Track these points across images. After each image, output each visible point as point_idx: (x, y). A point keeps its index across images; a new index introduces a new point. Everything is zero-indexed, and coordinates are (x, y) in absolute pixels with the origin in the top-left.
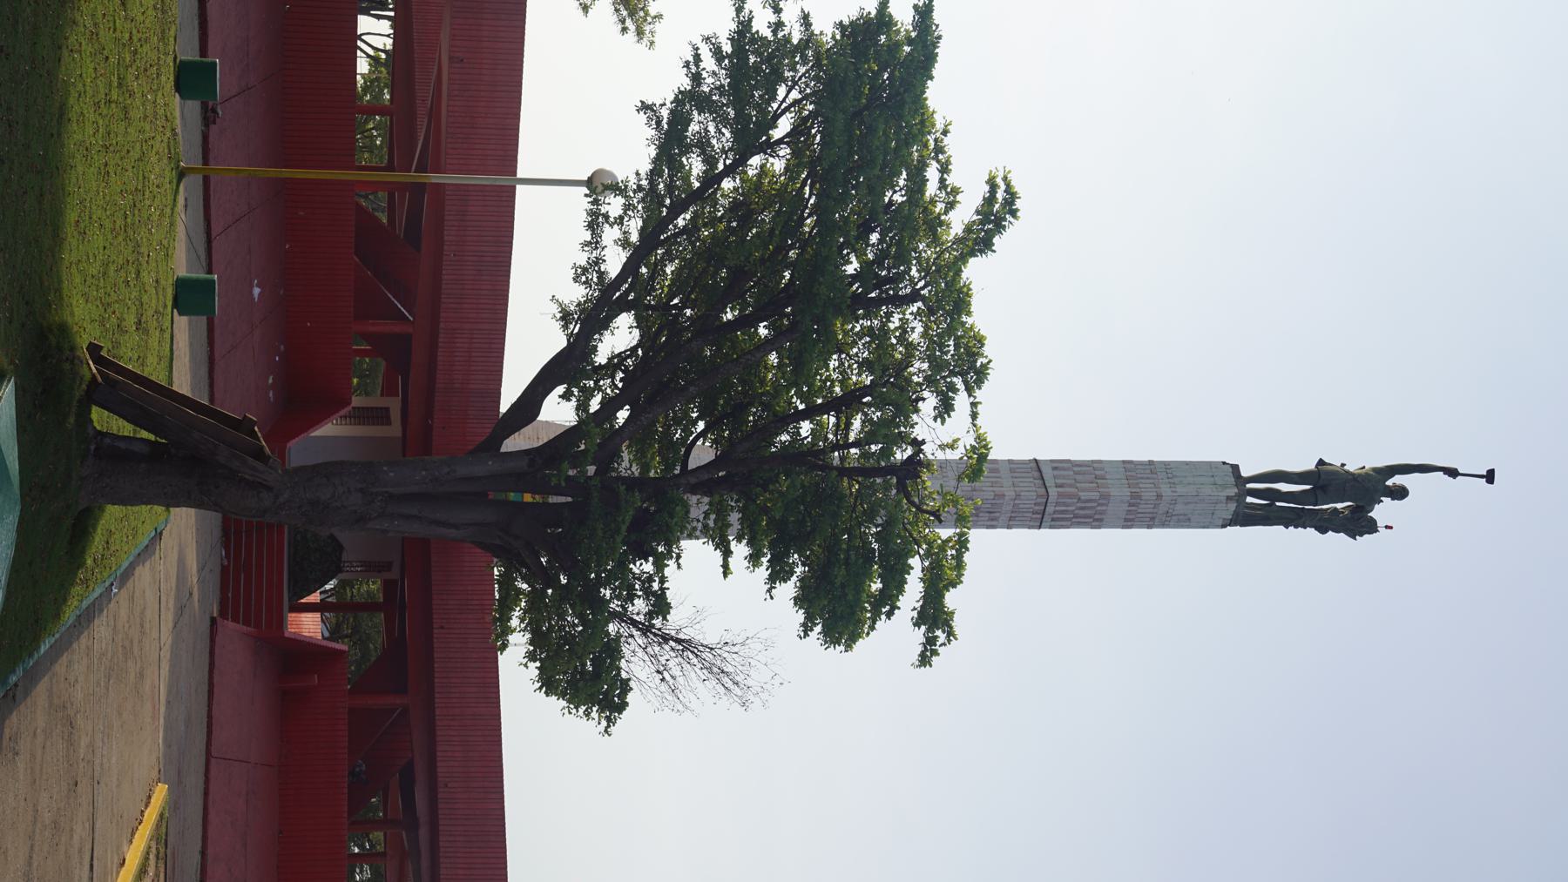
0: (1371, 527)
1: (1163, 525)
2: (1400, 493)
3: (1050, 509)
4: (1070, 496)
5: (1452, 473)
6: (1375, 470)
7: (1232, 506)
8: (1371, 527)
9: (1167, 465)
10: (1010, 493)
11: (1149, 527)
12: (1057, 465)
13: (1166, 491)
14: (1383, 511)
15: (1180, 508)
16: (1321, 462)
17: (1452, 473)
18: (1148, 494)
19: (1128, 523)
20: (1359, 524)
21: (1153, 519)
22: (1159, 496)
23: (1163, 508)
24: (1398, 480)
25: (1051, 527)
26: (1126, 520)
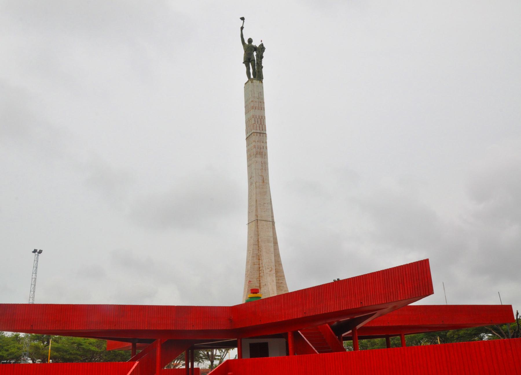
0: (262, 45)
1: (263, 99)
2: (250, 41)
3: (258, 131)
4: (253, 126)
5: (242, 28)
6: (244, 47)
7: (254, 81)
8: (262, 45)
9: (246, 102)
10: (254, 143)
11: (264, 103)
12: (247, 133)
13: (251, 100)
14: (256, 43)
15: (256, 95)
16: (244, 63)
17: (242, 28)
18: (252, 104)
19: (262, 109)
20: (261, 49)
21: (260, 102)
22: (252, 101)
23: (257, 100)
24: (246, 42)
25: (265, 130)
26: (261, 109)
